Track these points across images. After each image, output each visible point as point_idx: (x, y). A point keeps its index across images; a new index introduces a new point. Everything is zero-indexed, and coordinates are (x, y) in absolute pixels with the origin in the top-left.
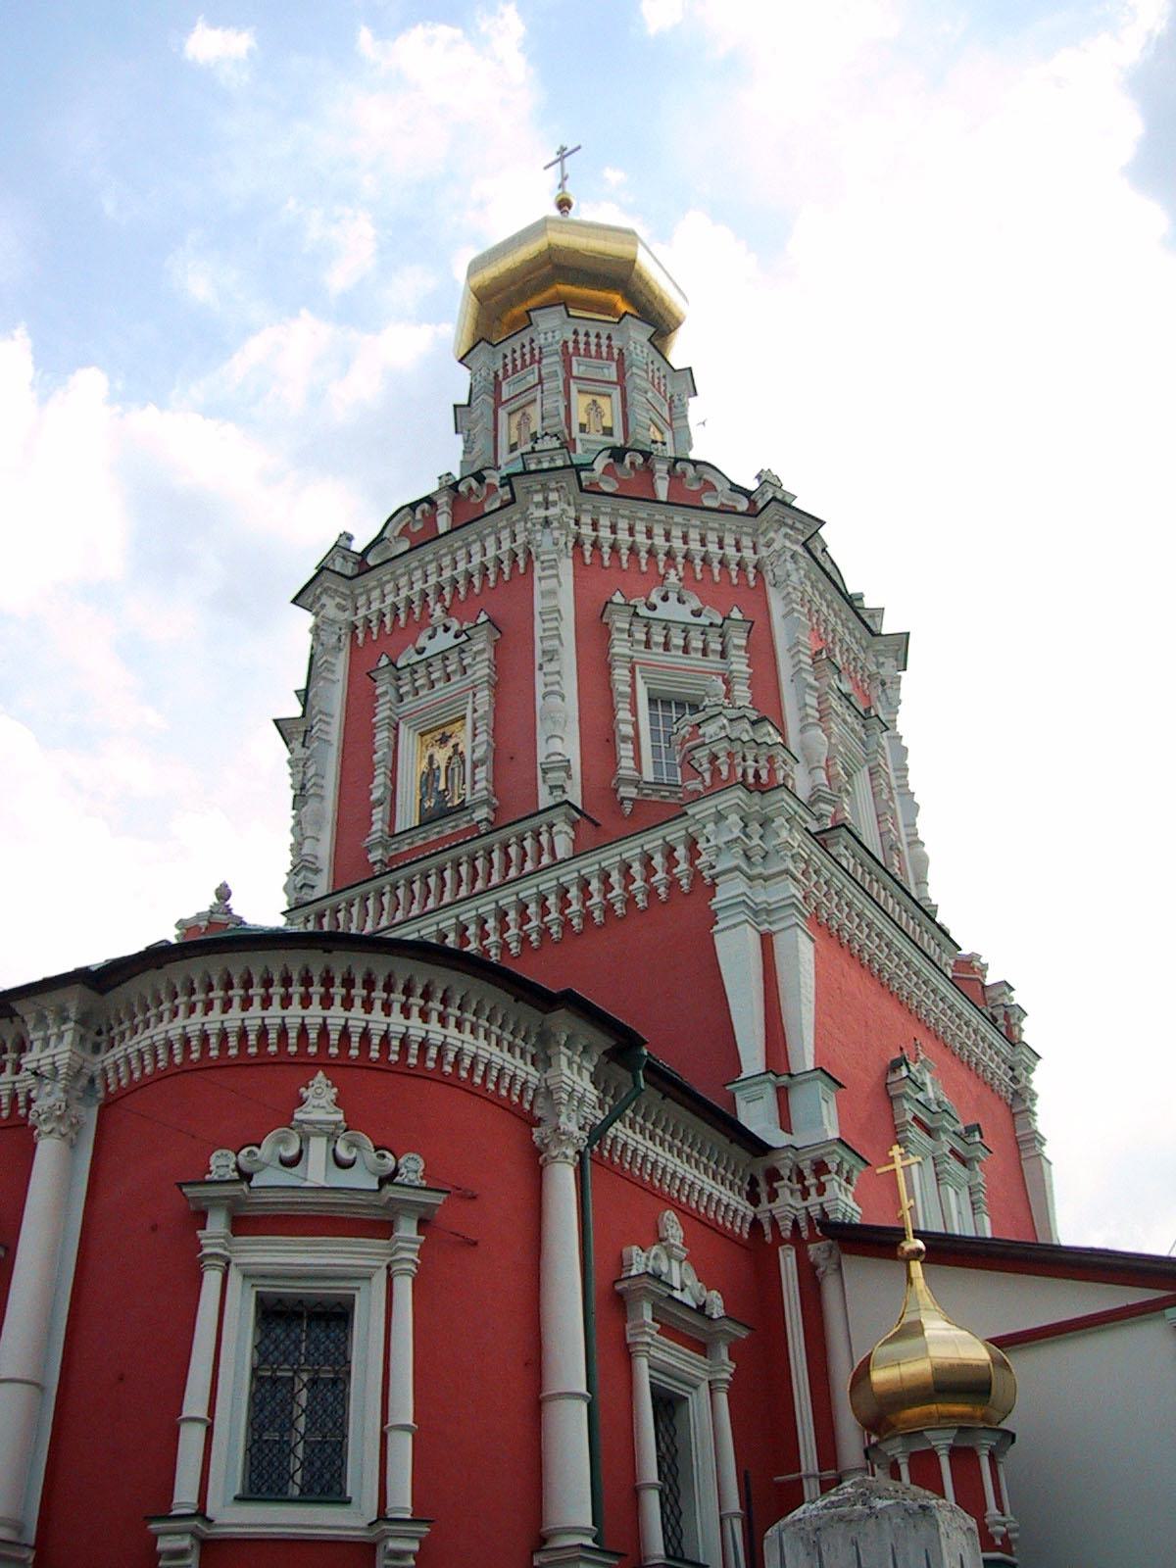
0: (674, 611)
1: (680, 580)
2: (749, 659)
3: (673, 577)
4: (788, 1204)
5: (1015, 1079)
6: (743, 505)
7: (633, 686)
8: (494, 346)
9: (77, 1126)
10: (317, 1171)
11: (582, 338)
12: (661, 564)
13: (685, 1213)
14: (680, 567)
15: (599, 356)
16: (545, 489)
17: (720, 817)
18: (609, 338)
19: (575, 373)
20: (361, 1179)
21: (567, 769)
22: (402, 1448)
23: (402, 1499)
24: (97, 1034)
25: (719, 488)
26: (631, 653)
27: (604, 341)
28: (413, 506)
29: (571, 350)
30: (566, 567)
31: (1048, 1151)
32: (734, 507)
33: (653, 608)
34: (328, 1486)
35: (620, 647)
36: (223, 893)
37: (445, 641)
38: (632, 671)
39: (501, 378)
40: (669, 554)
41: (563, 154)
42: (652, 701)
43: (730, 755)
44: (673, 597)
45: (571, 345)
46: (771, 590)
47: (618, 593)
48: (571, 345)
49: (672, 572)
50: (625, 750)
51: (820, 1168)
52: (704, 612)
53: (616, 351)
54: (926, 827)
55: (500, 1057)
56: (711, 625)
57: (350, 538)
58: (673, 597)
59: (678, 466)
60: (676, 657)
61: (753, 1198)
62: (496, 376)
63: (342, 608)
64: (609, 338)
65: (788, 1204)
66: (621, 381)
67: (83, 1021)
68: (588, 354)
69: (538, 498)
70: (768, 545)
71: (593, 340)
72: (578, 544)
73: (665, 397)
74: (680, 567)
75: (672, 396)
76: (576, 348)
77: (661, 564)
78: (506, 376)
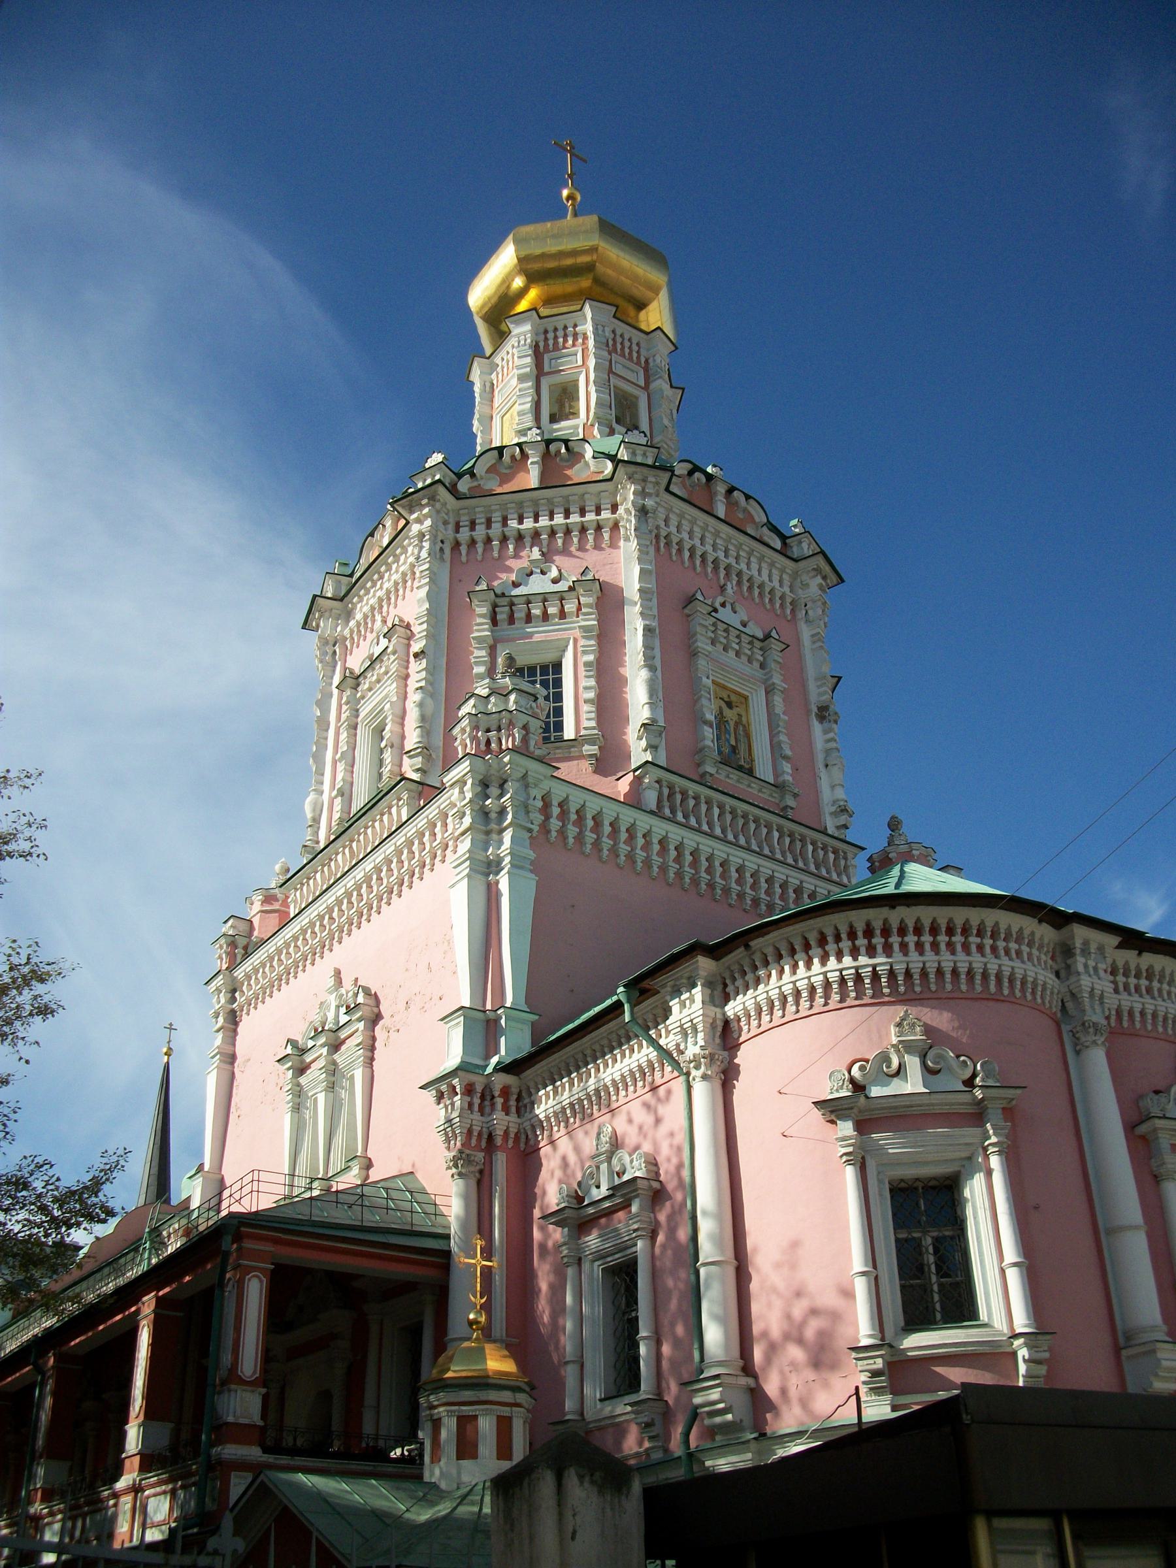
3: (729, 590)
6: (778, 544)
11: (619, 340)
15: (631, 359)
25: (757, 519)
40: (728, 568)
44: (728, 606)
52: (750, 624)
53: (643, 360)
58: (728, 606)
59: (736, 493)
66: (646, 388)
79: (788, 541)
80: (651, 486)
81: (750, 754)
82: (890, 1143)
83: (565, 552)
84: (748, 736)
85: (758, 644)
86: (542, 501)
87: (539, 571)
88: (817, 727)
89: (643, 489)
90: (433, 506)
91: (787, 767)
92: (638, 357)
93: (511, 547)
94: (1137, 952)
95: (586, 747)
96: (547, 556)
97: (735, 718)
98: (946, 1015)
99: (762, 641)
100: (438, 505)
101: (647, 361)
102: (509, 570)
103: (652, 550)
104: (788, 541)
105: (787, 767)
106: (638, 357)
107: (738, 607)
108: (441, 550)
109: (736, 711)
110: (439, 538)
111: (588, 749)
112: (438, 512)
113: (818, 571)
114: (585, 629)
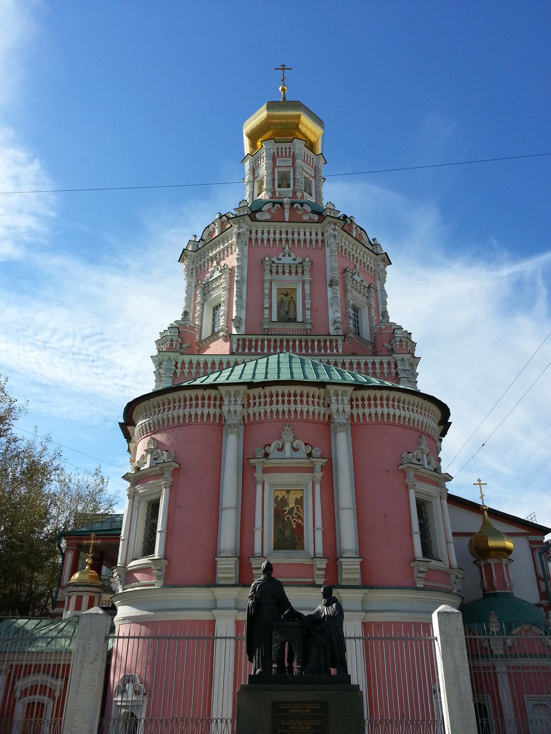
0: (287, 260)
1: (289, 249)
2: (310, 275)
3: (287, 248)
6: (316, 217)
8: (253, 156)
11: (280, 151)
12: (284, 244)
14: (290, 244)
15: (286, 156)
18: (290, 148)
19: (277, 165)
26: (270, 278)
27: (288, 150)
29: (276, 155)
32: (314, 219)
33: (280, 259)
35: (267, 277)
39: (255, 169)
40: (287, 240)
44: (287, 255)
45: (276, 154)
47: (267, 256)
48: (276, 154)
49: (287, 246)
50: (266, 312)
53: (292, 153)
56: (300, 263)
58: (287, 255)
59: (295, 206)
62: (253, 168)
64: (290, 148)
68: (282, 156)
71: (284, 150)
73: (312, 167)
74: (290, 244)
75: (315, 167)
76: (278, 155)
77: (284, 244)
78: (256, 168)
79: (323, 214)
80: (242, 223)
81: (296, 311)
82: (140, 489)
83: (224, 259)
84: (295, 305)
85: (300, 266)
86: (217, 242)
87: (216, 270)
88: (329, 289)
89: (239, 225)
90: (188, 258)
91: (308, 313)
92: (290, 154)
93: (210, 263)
94: (261, 388)
95: (221, 333)
96: (218, 263)
97: (290, 299)
98: (165, 435)
99: (302, 263)
100: (189, 257)
101: (294, 154)
102: (208, 272)
103: (246, 248)
104: (323, 214)
105: (308, 313)
106: (290, 154)
107: (291, 254)
108: (192, 272)
109: (289, 296)
110: (191, 269)
111: (221, 334)
112: (190, 259)
113: (330, 223)
114: (223, 288)
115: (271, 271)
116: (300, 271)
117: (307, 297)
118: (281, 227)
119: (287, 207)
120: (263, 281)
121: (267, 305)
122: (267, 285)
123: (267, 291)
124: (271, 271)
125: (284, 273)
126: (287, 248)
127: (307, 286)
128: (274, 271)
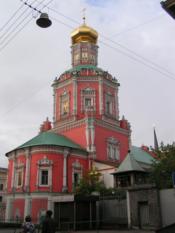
0: (88, 89)
3: (88, 85)
4: (90, 157)
5: (128, 134)
7: (83, 100)
9: (29, 158)
10: (45, 163)
13: (78, 159)
16: (74, 77)
17: (87, 119)
20: (48, 163)
21: (76, 111)
22: (51, 181)
23: (51, 185)
24: (30, 150)
27: (86, 45)
28: (63, 75)
30: (77, 85)
31: (132, 141)
34: (47, 183)
35: (82, 95)
36: (48, 118)
37: (65, 93)
38: (83, 98)
41: (85, 10)
42: (86, 100)
43: (88, 112)
44: (88, 87)
46: (99, 85)
51: (92, 153)
54: (119, 107)
55: (59, 151)
57: (57, 78)
58: (88, 87)
60: (88, 95)
61: (87, 156)
63: (56, 87)
65: (90, 157)
67: (29, 149)
69: (73, 78)
70: (99, 79)
71: (85, 45)
72: (78, 82)
115: (83, 93)
116: (92, 93)
117: (95, 102)
118: (86, 78)
119: (88, 70)
120: (80, 97)
121: (82, 105)
122: (82, 98)
123: (82, 100)
124: (83, 93)
125: (87, 94)
126: (88, 85)
127: (95, 98)
128: (84, 93)
